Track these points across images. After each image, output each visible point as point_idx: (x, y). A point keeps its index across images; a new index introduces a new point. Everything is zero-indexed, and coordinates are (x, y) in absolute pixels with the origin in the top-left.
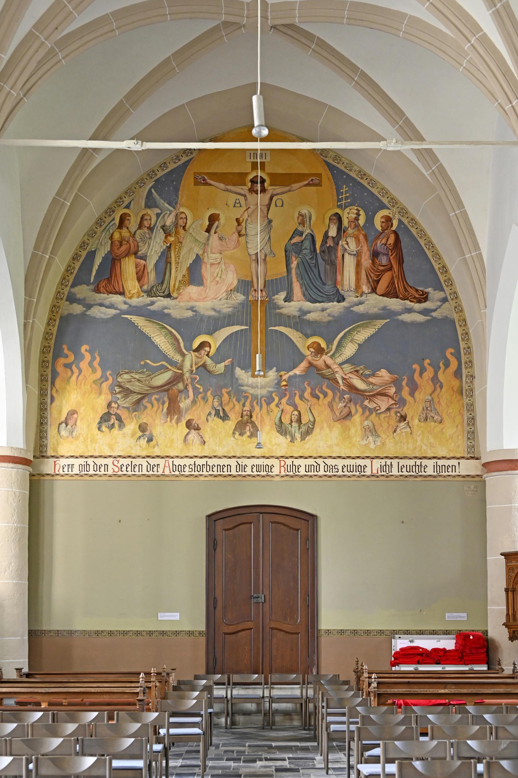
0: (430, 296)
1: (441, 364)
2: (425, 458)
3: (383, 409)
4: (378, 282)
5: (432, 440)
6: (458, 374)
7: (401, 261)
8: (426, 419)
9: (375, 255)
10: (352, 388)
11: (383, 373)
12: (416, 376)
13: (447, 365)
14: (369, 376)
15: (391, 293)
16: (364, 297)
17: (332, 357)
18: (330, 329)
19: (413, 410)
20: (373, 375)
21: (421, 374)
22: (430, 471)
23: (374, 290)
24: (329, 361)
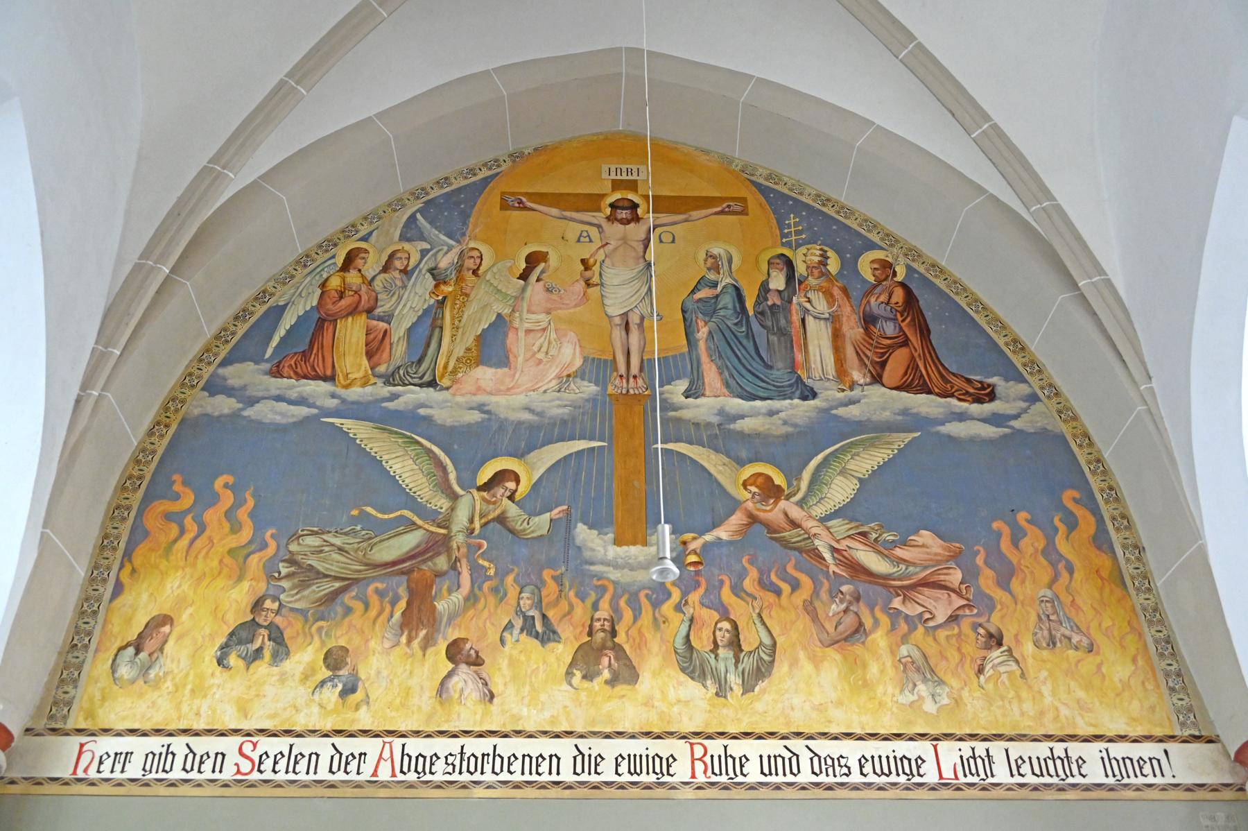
0: (998, 390)
1: (1056, 521)
2: (1073, 738)
3: (941, 619)
4: (883, 364)
5: (1081, 694)
6: (1101, 541)
7: (924, 331)
8: (1052, 642)
9: (869, 320)
10: (857, 570)
11: (925, 537)
12: (1005, 544)
13: (1072, 524)
14: (894, 544)
15: (913, 383)
16: (857, 392)
17: (801, 504)
18: (793, 449)
19: (1014, 620)
20: (904, 543)
21: (1015, 543)
23: (877, 379)
24: (796, 513)
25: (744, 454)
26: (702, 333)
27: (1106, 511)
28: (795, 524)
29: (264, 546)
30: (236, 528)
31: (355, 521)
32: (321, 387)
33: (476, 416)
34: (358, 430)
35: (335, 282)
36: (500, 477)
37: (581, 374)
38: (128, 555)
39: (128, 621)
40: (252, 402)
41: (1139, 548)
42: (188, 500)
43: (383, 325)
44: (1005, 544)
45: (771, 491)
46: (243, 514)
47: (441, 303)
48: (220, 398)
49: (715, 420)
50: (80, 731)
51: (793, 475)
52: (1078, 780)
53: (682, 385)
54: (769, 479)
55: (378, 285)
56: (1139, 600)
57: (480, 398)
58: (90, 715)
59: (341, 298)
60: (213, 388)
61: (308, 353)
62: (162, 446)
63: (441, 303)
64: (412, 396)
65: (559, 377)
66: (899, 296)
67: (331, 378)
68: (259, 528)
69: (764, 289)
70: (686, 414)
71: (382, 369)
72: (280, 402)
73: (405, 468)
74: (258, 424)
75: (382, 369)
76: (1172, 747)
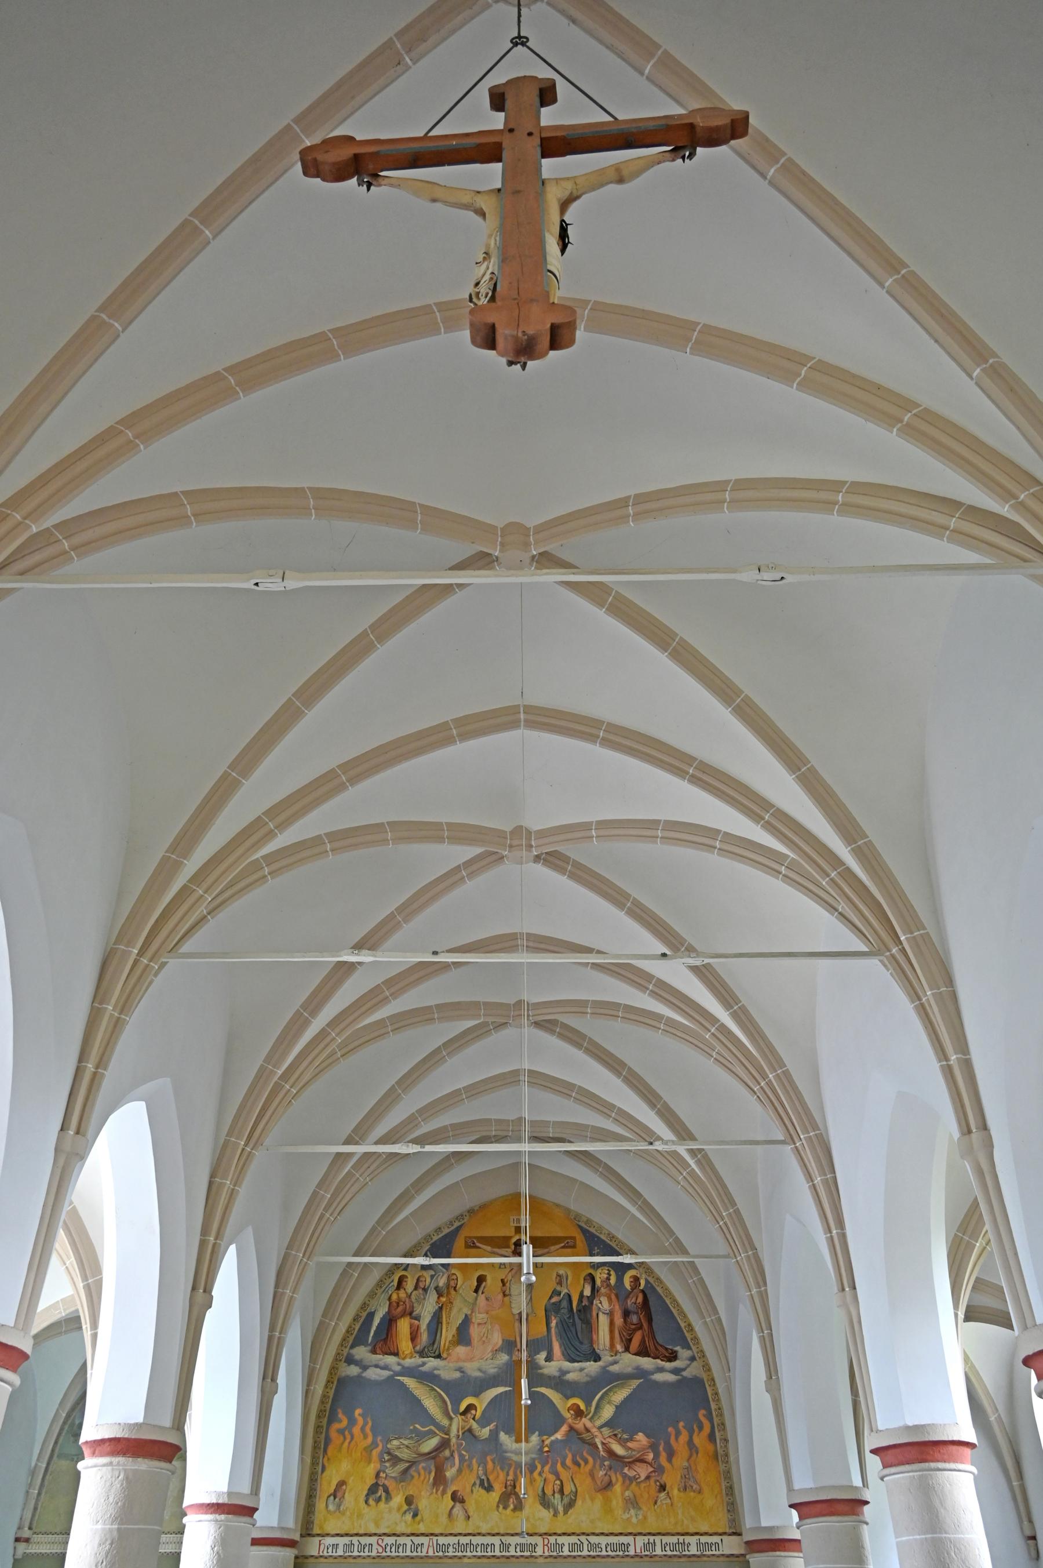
0: (679, 1355)
1: (695, 1427)
2: (687, 1534)
3: (643, 1478)
4: (630, 1340)
5: (693, 1513)
6: (712, 1437)
7: (650, 1321)
8: (685, 1489)
9: (626, 1314)
10: (611, 1453)
11: (640, 1436)
12: (673, 1438)
13: (701, 1428)
14: (627, 1440)
15: (643, 1352)
16: (618, 1357)
17: (591, 1419)
18: (588, 1390)
19: (672, 1478)
20: (631, 1439)
21: (677, 1439)
22: (693, 1550)
23: (627, 1349)
24: (589, 1425)
25: (569, 1393)
26: (553, 1324)
27: (716, 1420)
28: (588, 1430)
29: (377, 1446)
30: (366, 1437)
31: (411, 1432)
32: (390, 1360)
33: (458, 1375)
34: (410, 1382)
35: (394, 1297)
36: (470, 1407)
37: (500, 1350)
38: (325, 1451)
39: (329, 1483)
40: (365, 1368)
41: (726, 1440)
42: (345, 1422)
43: (416, 1322)
44: (673, 1438)
45: (579, 1413)
46: (368, 1429)
47: (441, 1308)
48: (352, 1366)
49: (557, 1374)
50: (318, 1535)
51: (588, 1404)
52: (687, 1553)
53: (543, 1355)
54: (578, 1406)
55: (413, 1297)
56: (722, 1467)
57: (461, 1364)
58: (321, 1528)
59: (398, 1306)
60: (350, 1360)
61: (385, 1341)
62: (331, 1394)
63: (441, 1308)
64: (432, 1363)
65: (492, 1351)
66: (640, 1299)
67: (396, 1354)
68: (375, 1436)
69: (581, 1295)
70: (545, 1371)
71: (418, 1348)
72: (379, 1368)
73: (430, 1404)
74: (369, 1381)
75: (418, 1348)
76: (724, 1538)
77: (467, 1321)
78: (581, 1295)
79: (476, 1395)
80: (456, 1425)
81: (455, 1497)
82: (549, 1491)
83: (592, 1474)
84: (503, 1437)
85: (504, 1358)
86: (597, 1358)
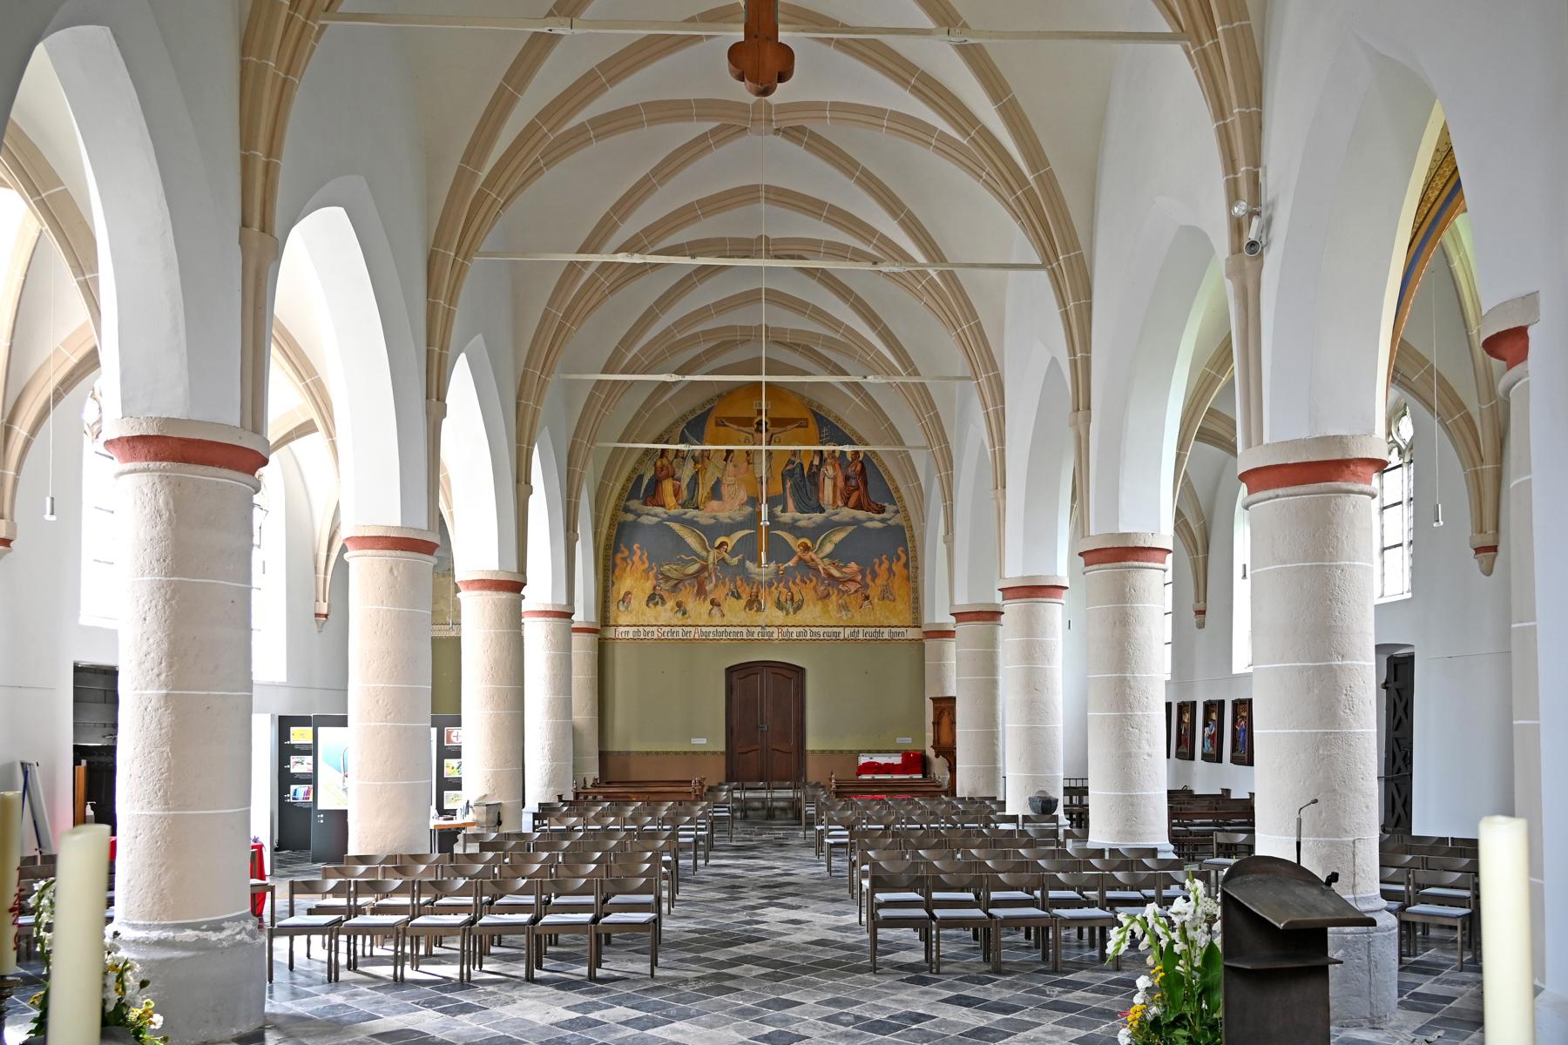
37: (747, 503)
45: (806, 548)
51: (814, 542)
77: (718, 482)
78: (811, 464)
79: (728, 535)
80: (712, 556)
81: (712, 602)
82: (783, 599)
83: (815, 589)
84: (748, 564)
85: (750, 509)
86: (822, 511)
